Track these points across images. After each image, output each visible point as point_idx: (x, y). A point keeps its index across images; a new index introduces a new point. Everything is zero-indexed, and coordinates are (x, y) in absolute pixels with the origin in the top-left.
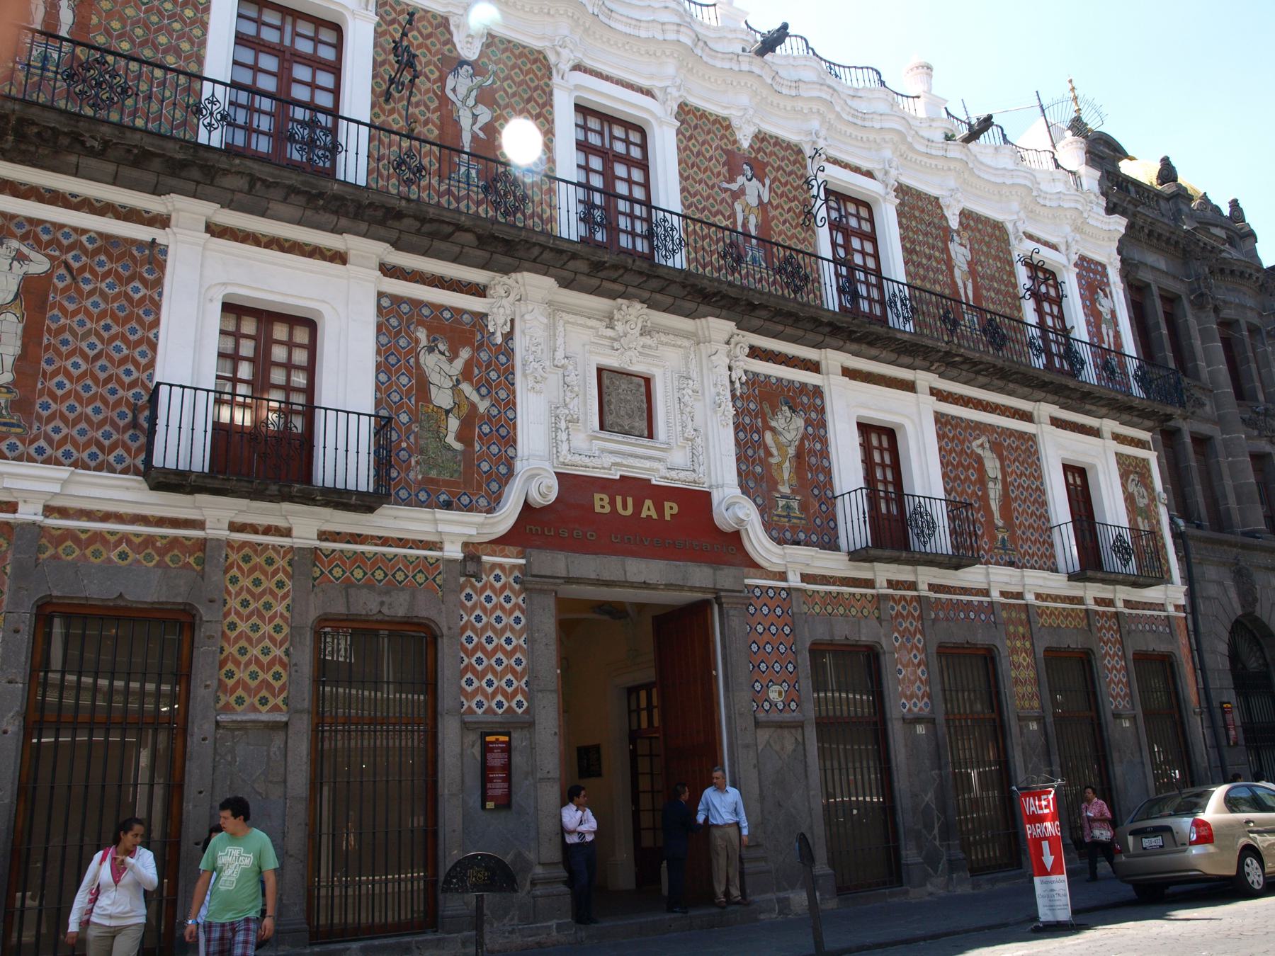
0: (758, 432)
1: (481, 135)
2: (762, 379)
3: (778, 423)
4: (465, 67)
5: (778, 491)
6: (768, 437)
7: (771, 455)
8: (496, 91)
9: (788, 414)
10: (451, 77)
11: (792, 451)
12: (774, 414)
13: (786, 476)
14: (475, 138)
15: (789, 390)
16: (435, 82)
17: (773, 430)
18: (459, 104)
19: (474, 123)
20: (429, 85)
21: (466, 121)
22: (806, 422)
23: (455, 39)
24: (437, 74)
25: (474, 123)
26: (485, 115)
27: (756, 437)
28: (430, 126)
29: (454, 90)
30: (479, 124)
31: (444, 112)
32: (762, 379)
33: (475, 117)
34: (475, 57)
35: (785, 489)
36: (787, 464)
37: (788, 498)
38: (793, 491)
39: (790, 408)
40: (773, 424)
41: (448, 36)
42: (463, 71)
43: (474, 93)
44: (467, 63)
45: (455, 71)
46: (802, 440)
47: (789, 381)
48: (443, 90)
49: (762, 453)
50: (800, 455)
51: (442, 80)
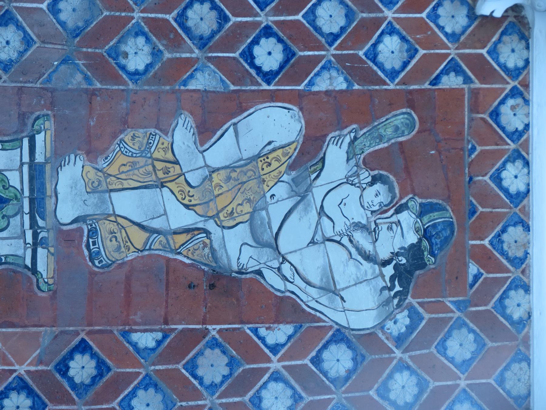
0: (293, 67)
5: (58, 157)
6: (275, 125)
7: (206, 132)
9: (388, 244)
11: (236, 248)
13: (127, 204)
15: (484, 258)
17: (308, 156)
27: (268, 54)
32: (511, 119)
36: (181, 218)
37: (37, 205)
39: (414, 252)
40: (336, 156)
46: (285, 308)
47: (522, 261)
49: (204, 81)
50: (227, 293)
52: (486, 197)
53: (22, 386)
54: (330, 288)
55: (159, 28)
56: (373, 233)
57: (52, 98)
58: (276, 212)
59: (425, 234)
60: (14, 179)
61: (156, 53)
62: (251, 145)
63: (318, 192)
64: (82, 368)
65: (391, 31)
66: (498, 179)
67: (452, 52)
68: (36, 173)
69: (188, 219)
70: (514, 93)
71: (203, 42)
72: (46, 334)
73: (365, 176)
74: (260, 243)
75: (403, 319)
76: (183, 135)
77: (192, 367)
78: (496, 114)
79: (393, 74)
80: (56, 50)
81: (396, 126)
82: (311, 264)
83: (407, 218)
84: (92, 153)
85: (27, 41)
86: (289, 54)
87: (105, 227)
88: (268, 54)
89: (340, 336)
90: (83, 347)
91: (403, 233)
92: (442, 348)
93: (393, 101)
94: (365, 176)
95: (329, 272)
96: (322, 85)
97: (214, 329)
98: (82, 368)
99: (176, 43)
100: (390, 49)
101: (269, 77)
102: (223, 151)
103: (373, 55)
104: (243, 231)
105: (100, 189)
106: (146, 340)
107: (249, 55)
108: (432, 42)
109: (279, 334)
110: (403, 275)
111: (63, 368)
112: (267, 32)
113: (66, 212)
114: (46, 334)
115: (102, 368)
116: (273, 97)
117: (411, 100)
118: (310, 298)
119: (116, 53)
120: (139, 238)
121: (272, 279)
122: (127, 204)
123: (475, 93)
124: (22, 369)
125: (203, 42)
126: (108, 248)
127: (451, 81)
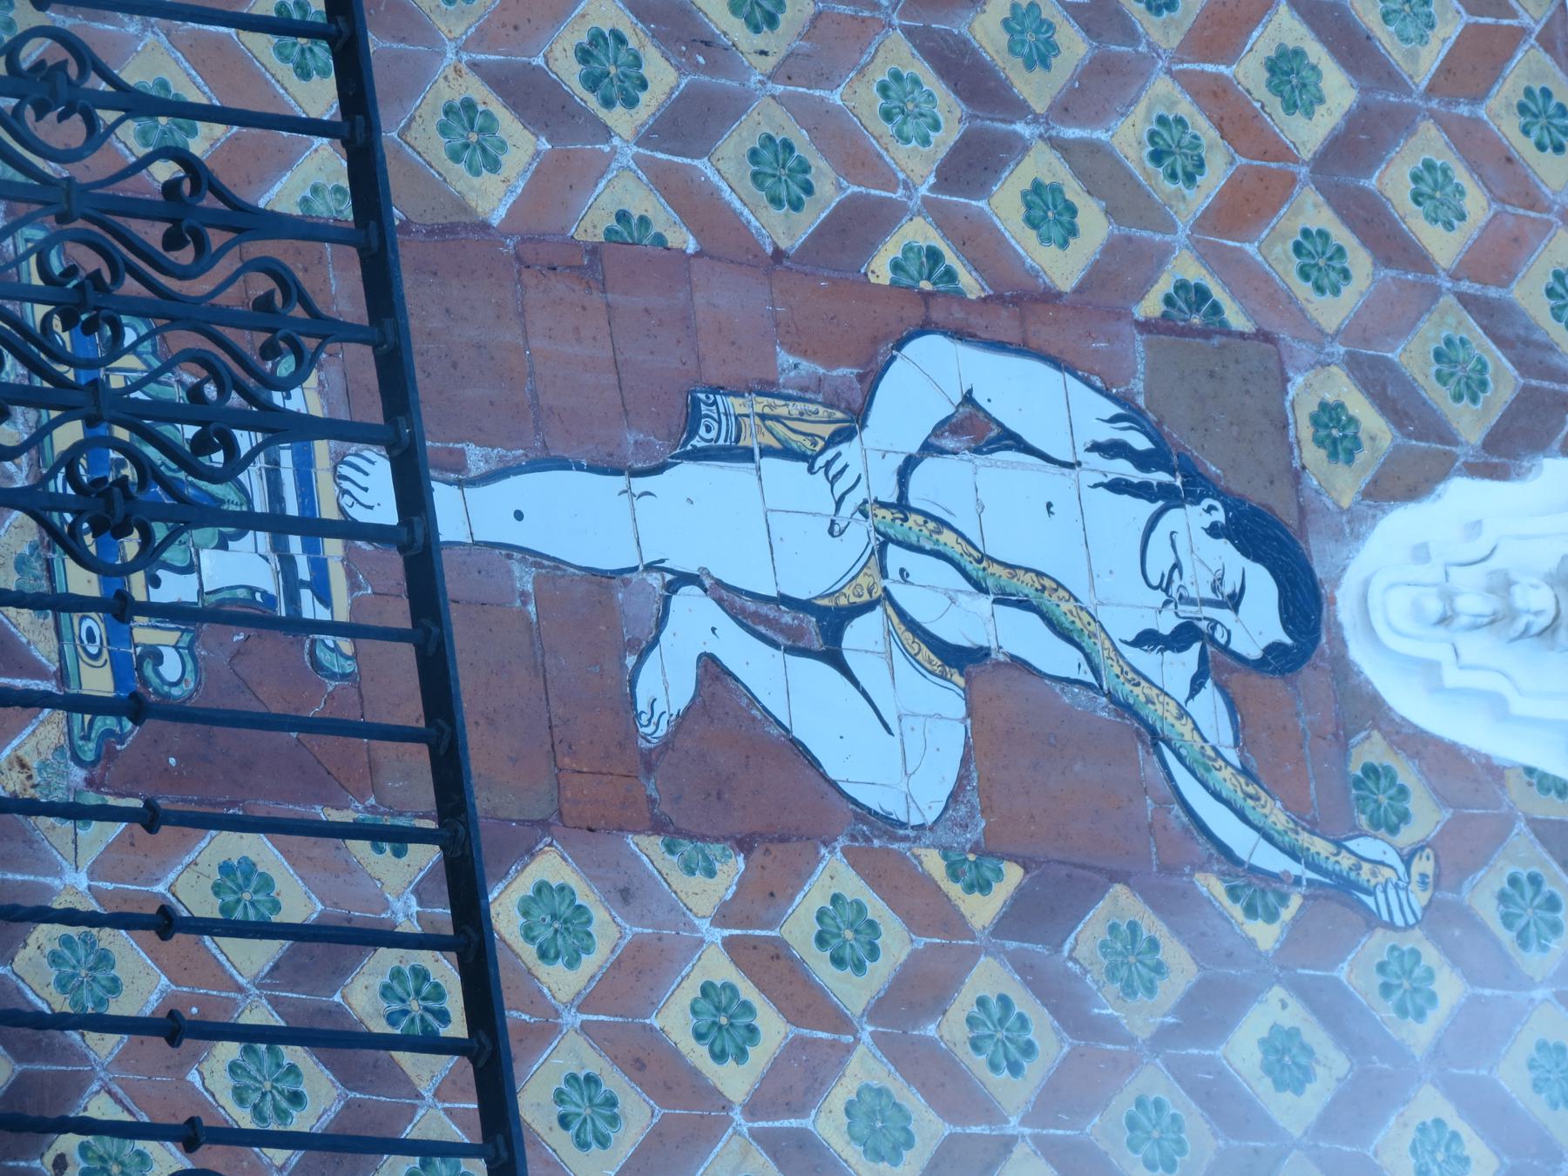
1: (665, 687)
4: (1262, 588)
8: (1170, 899)
10: (1094, 415)
14: (606, 612)
16: (978, 241)
18: (870, 460)
19: (753, 613)
20: (916, 165)
21: (738, 517)
23: (1463, 496)
24: (1062, 267)
25: (753, 613)
26: (884, 738)
28: (522, 146)
29: (975, 430)
30: (759, 667)
31: (726, 298)
33: (818, 630)
34: (1408, 702)
41: (1471, 424)
42: (1193, 539)
43: (1057, 659)
44: (1303, 602)
45: (1165, 471)
48: (927, 310)
51: (1016, 317)
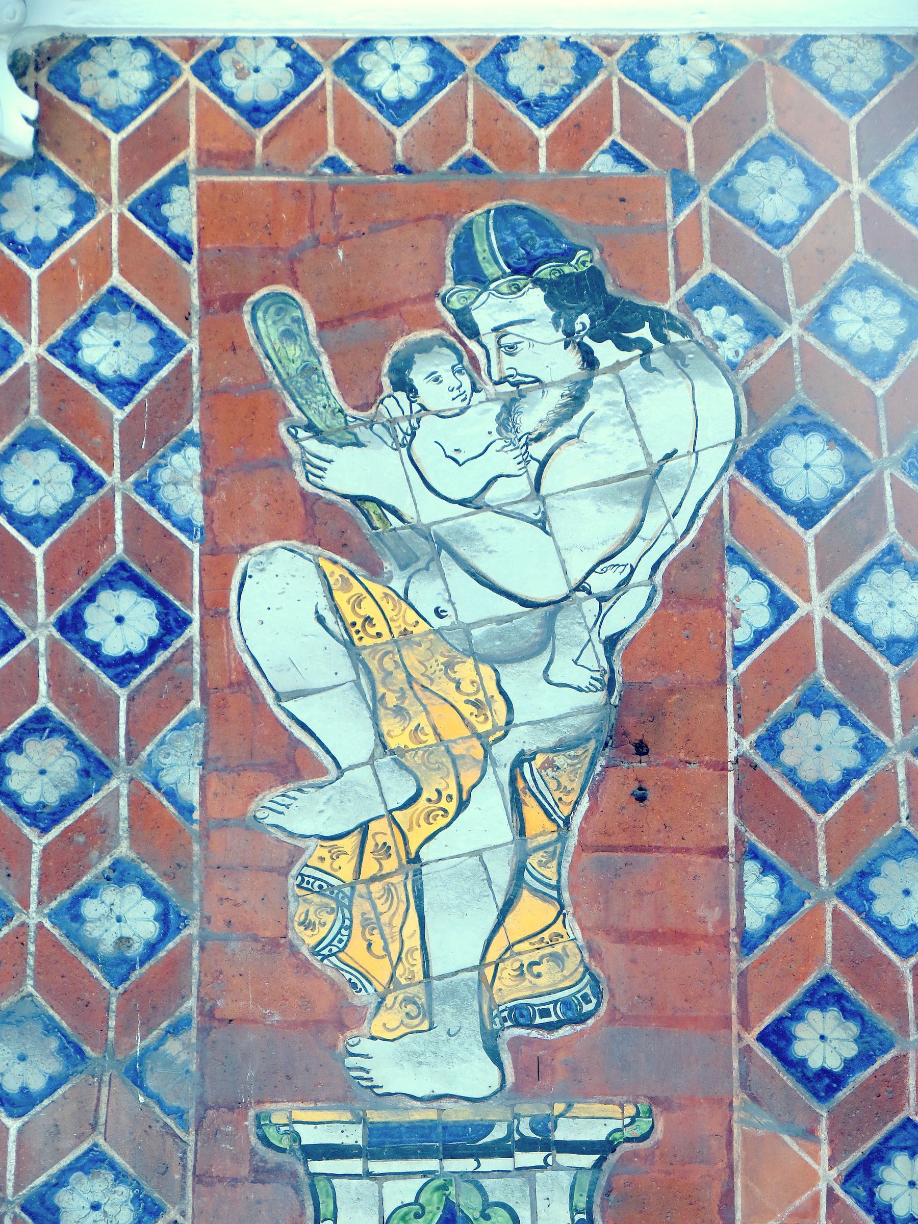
2: (268, 78)
3: (430, 453)
5: (356, 1092)
6: (279, 608)
7: (293, 761)
11: (558, 696)
12: (373, 380)
15: (577, 140)
17: (349, 533)
22: (753, 396)
27: (123, 622)
32: (268, 78)
35: (436, 1067)
38: (531, 1074)
39: (565, 294)
40: (353, 471)
46: (690, 587)
49: (181, 768)
52: (443, 137)
53: (864, 1175)
54: (646, 484)
55: (62, 868)
56: (522, 386)
57: (220, 1107)
58: (474, 604)
59: (524, 269)
60: (400, 1193)
61: (120, 875)
62: (327, 662)
63: (431, 511)
64: (824, 1041)
65: (69, 347)
66: (400, 109)
67: (115, 210)
68: (386, 1143)
69: (490, 802)
70: (208, 70)
71: (95, 769)
72: (747, 1121)
73: (394, 405)
74: (546, 640)
75: (714, 320)
76: (305, 814)
77: (822, 794)
78: (256, 113)
79: (166, 343)
80: (115, 1100)
81: (281, 337)
82: (590, 527)
83: (488, 313)
84: (344, 1018)
85: (93, 1161)
86: (122, 576)
87: (509, 989)
88: (123, 622)
89: (753, 462)
90: (777, 1038)
91: (522, 320)
92: (777, 233)
93: (227, 344)
94: (394, 405)
95: (605, 488)
96: (189, 501)
97: (738, 745)
98: (824, 1041)
99: (97, 830)
100: (111, 349)
101: (172, 622)
102: (338, 725)
103: (124, 388)
104: (517, 679)
105: (427, 997)
106: (761, 897)
107: (124, 667)
108: (95, 258)
109: (748, 600)
110: (616, 320)
111: (825, 1083)
112: (71, 625)
113: (475, 1075)
114: (747, 1121)
115: (824, 995)
116: (217, 611)
117: (225, 303)
118: (667, 529)
119: (119, 966)
120: (532, 913)
121: (624, 614)
122: (457, 942)
123: (210, 159)
124: (827, 1176)
125: (95, 769)
126: (556, 980)
127: (182, 212)
